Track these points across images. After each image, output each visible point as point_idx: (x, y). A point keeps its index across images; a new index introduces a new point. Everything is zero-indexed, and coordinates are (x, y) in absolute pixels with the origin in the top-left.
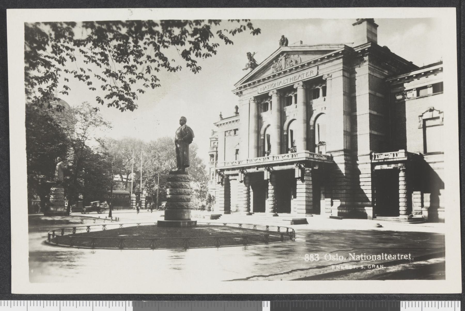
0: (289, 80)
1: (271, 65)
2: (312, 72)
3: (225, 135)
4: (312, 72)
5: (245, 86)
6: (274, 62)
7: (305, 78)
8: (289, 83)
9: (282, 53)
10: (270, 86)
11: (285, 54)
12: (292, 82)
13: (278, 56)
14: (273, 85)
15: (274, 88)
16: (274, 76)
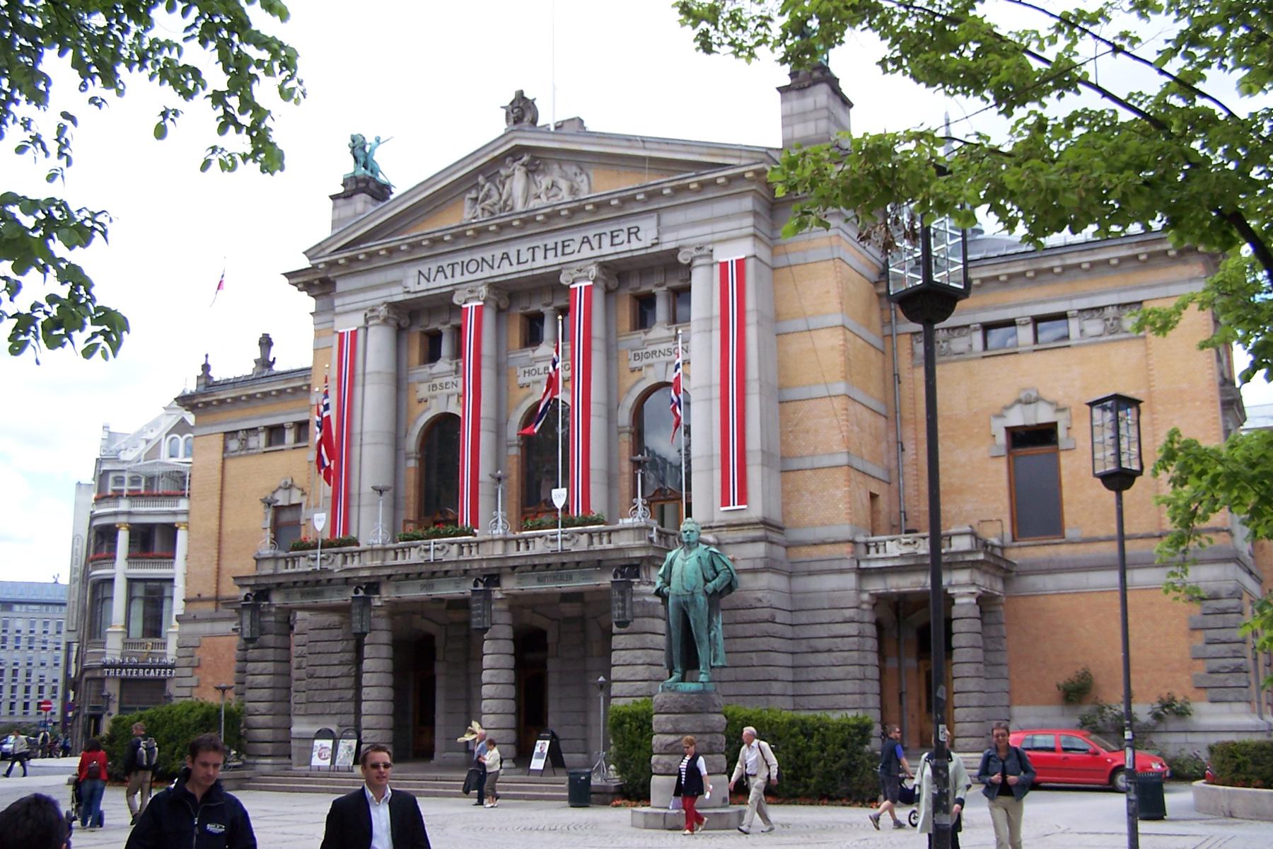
0: (539, 254)
1: (468, 190)
3: (225, 448)
5: (352, 260)
6: (481, 179)
7: (607, 249)
8: (540, 262)
9: (516, 153)
10: (458, 269)
11: (526, 158)
12: (551, 260)
13: (499, 161)
14: (473, 267)
15: (479, 275)
16: (480, 232)
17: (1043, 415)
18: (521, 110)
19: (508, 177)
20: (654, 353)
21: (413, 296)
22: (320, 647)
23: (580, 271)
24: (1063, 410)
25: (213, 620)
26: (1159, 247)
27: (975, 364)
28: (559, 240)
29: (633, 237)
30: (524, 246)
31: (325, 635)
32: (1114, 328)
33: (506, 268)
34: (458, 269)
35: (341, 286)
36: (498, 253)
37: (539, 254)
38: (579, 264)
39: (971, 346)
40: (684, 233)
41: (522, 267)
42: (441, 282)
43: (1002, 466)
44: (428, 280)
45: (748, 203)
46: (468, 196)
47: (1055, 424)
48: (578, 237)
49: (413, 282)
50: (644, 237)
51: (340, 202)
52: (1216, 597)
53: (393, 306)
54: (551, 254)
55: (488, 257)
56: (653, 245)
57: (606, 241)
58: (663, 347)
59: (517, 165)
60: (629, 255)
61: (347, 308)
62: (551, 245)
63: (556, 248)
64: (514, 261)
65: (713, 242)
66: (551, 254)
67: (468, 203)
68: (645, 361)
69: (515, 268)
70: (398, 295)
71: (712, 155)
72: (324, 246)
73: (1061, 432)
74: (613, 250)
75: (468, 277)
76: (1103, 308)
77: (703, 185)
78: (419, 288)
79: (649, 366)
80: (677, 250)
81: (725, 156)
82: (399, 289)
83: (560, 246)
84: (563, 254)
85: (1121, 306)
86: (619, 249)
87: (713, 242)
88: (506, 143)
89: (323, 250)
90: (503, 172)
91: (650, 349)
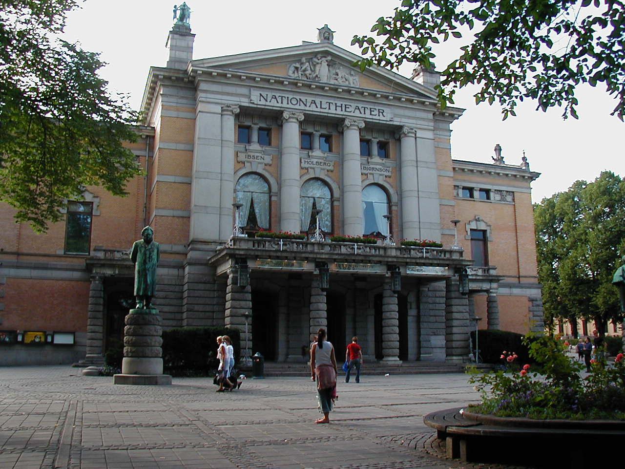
0: (333, 107)
1: (295, 62)
2: (381, 112)
4: (381, 112)
7: (368, 115)
8: (332, 110)
9: (326, 53)
10: (285, 101)
11: (329, 58)
12: (339, 111)
13: (316, 54)
14: (294, 102)
15: (297, 107)
17: (482, 227)
18: (326, 34)
19: (318, 63)
20: (373, 168)
21: (255, 106)
22: (197, 294)
23: (355, 122)
24: (490, 226)
25: (18, 267)
26: (523, 174)
27: (460, 201)
28: (344, 104)
29: (380, 114)
30: (324, 101)
31: (201, 286)
32: (503, 199)
33: (313, 107)
34: (285, 101)
35: (203, 86)
36: (310, 99)
37: (333, 107)
38: (355, 118)
39: (458, 194)
40: (404, 120)
41: (322, 110)
42: (274, 105)
43: (469, 243)
44: (266, 101)
45: (431, 116)
46: (294, 65)
47: (484, 232)
48: (354, 105)
49: (257, 99)
50: (388, 116)
51: (176, 36)
52: (537, 301)
53: (241, 107)
54: (339, 109)
55: (303, 99)
56: (390, 121)
57: (368, 112)
58: (378, 167)
59: (323, 59)
60: (378, 121)
61: (208, 100)
62: (339, 104)
63: (341, 107)
64: (319, 106)
65: (417, 128)
66: (339, 109)
67: (292, 69)
68: (369, 171)
69: (319, 110)
70: (245, 103)
71: (425, 91)
72: (204, 61)
73: (488, 234)
74: (371, 117)
75: (290, 106)
76: (501, 191)
77: (419, 102)
78: (260, 103)
79: (370, 174)
80: (400, 128)
81: (430, 94)
82: (246, 100)
83: (343, 106)
84: (346, 111)
85: (507, 192)
86: (374, 117)
87: (417, 128)
88: (322, 47)
89: (203, 64)
90: (315, 60)
91: (372, 166)
